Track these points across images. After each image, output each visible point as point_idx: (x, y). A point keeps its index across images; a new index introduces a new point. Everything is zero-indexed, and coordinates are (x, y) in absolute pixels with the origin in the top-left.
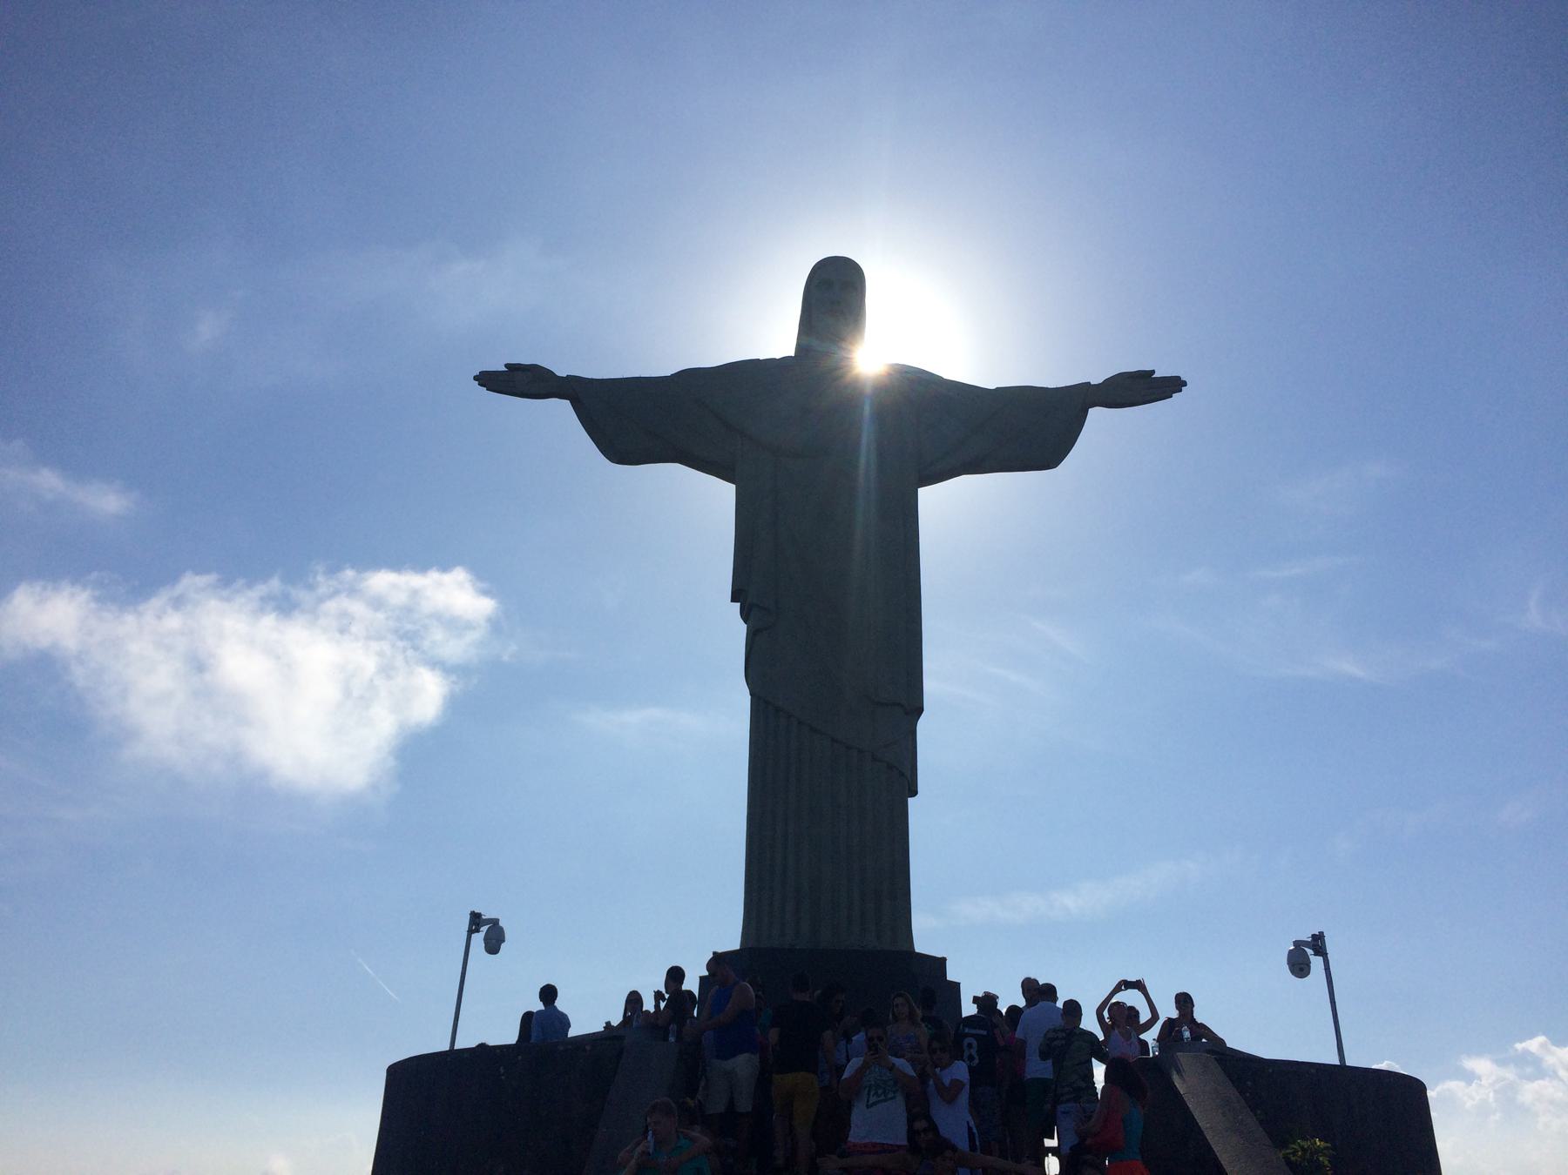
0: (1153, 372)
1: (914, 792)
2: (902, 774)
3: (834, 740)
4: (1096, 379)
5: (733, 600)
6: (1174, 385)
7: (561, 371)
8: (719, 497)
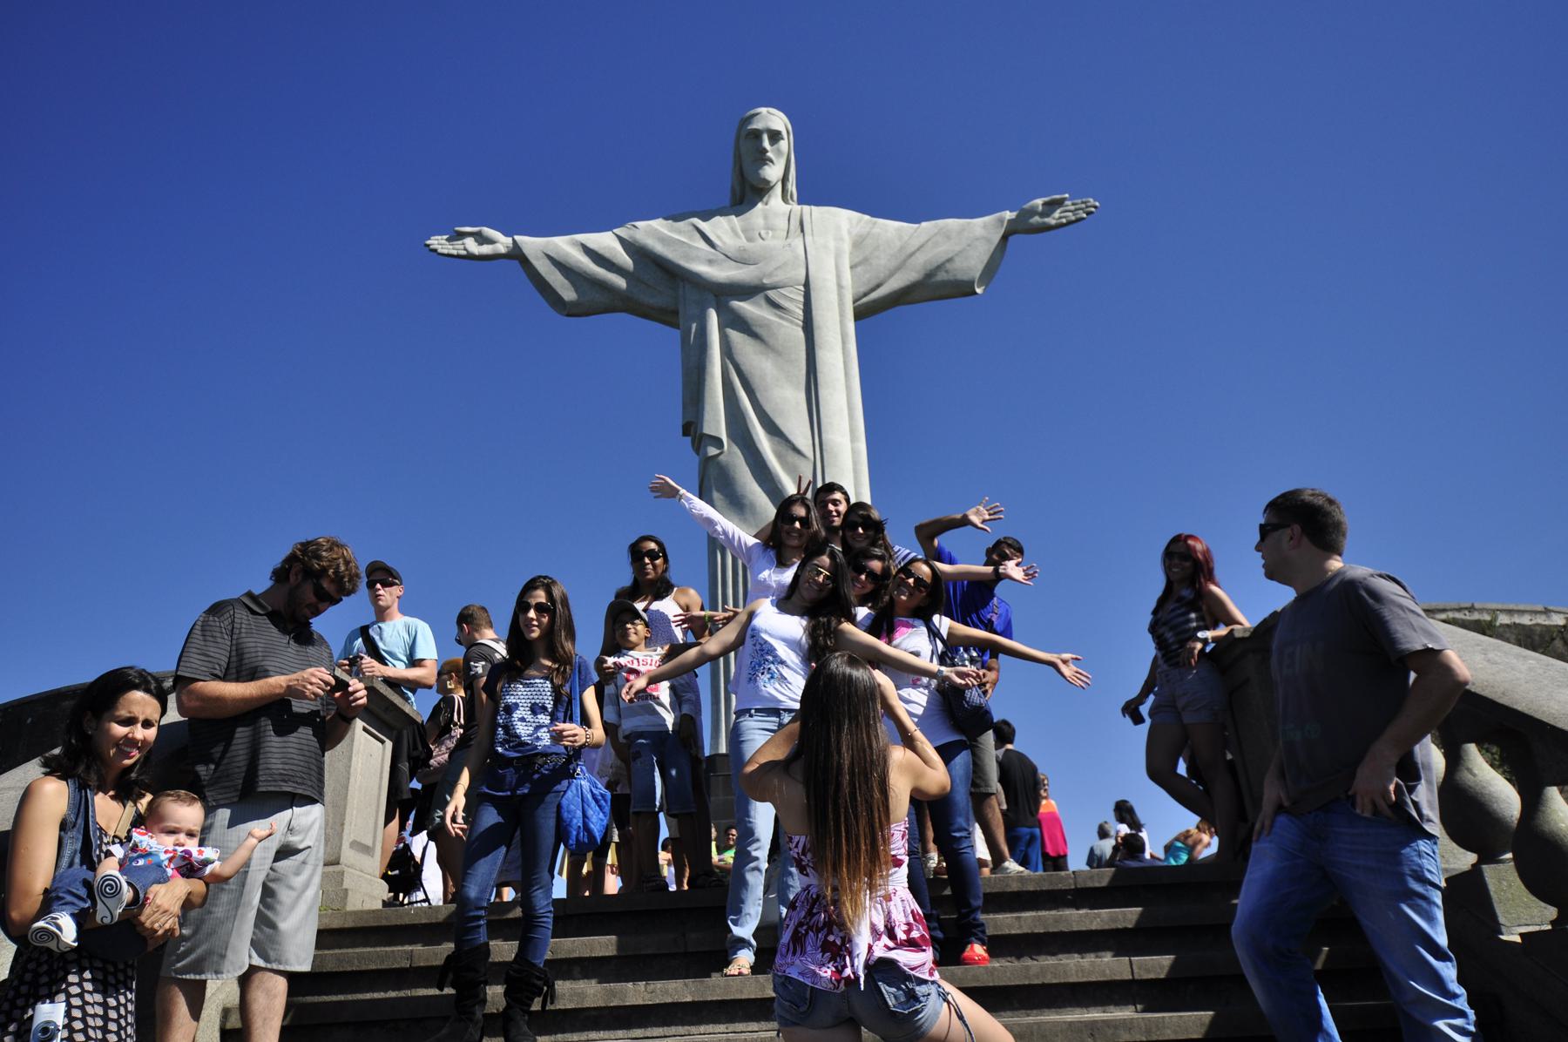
5: (686, 432)
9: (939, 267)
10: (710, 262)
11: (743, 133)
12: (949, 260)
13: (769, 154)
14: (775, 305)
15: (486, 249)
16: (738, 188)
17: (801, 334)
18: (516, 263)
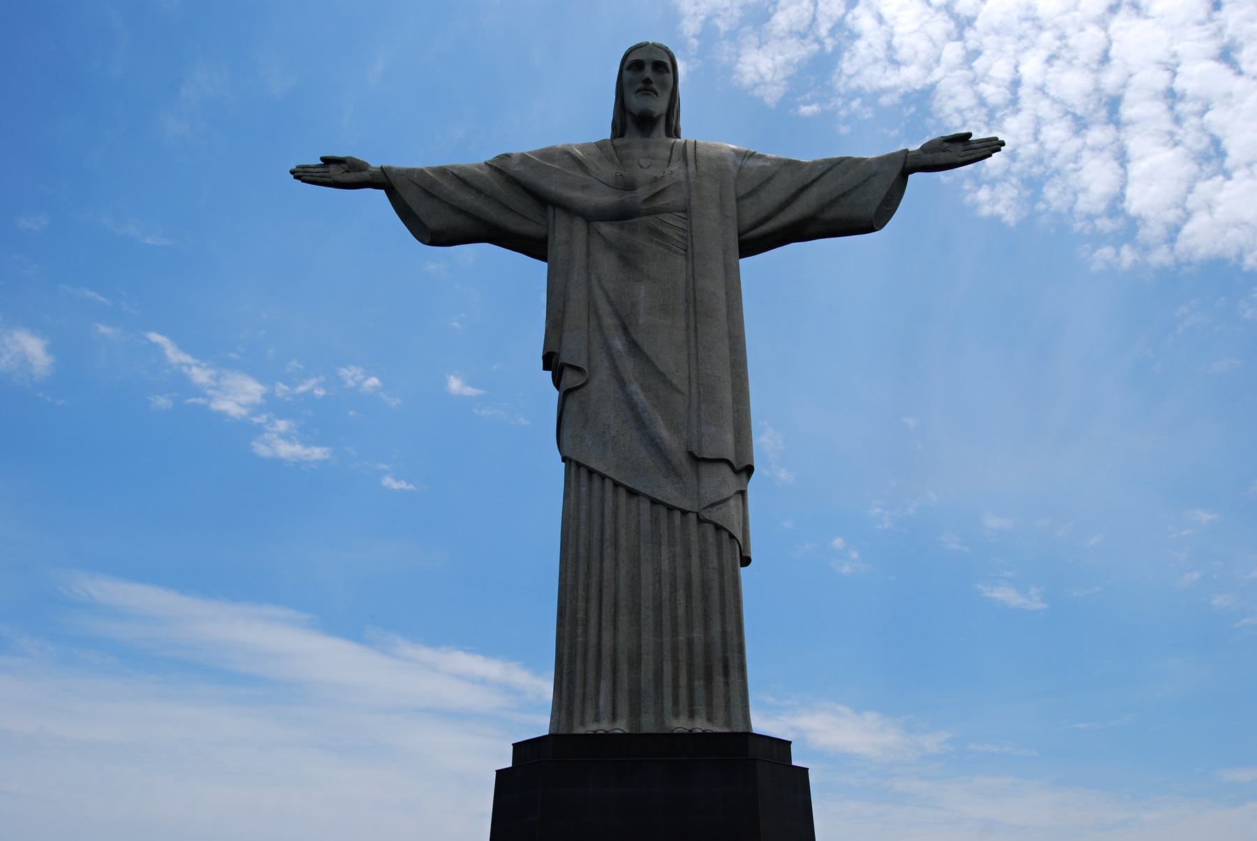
0: (970, 135)
1: (746, 561)
2: (732, 536)
3: (654, 502)
4: (915, 147)
6: (994, 146)
7: (375, 162)
8: (529, 275)
9: (833, 202)
10: (584, 188)
11: (627, 64)
12: (843, 195)
13: (654, 86)
14: (654, 232)
15: (352, 177)
16: (618, 121)
17: (680, 260)
18: (382, 193)
